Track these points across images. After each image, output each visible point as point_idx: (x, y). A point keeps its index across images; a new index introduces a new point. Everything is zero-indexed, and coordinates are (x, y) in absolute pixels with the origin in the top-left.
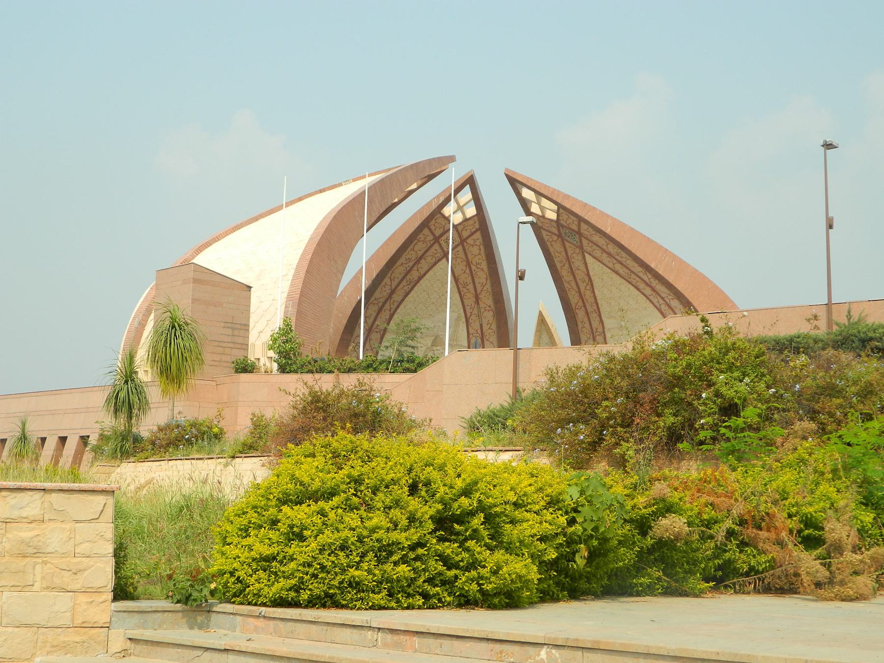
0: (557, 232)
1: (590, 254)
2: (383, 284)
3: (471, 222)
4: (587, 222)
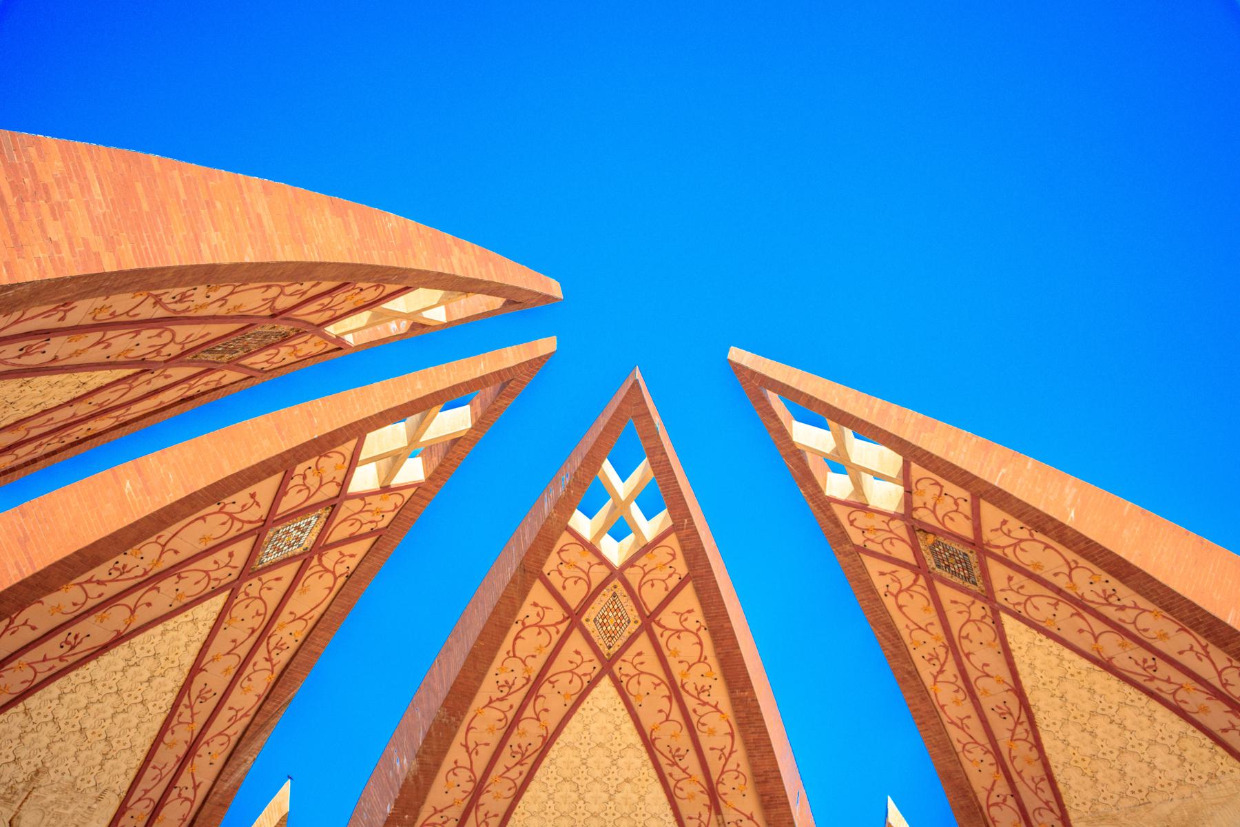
0: (909, 557)
1: (1017, 616)
2: (447, 764)
3: (661, 554)
4: (1002, 499)
